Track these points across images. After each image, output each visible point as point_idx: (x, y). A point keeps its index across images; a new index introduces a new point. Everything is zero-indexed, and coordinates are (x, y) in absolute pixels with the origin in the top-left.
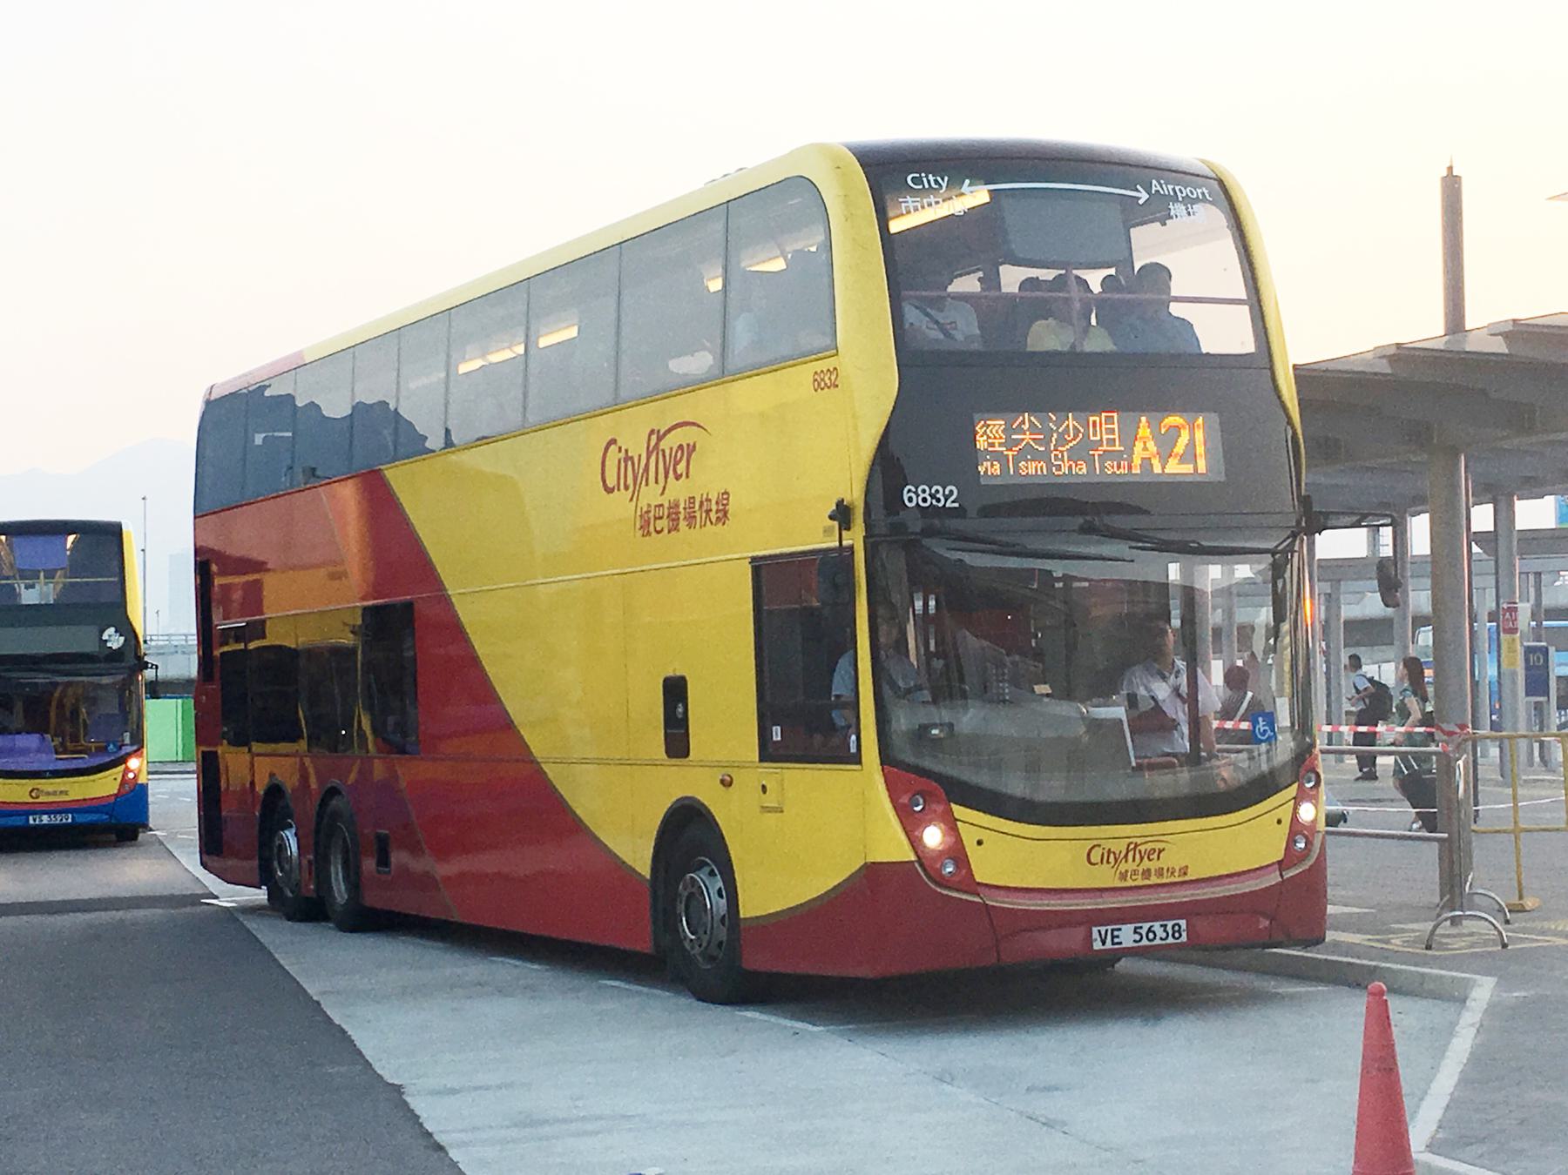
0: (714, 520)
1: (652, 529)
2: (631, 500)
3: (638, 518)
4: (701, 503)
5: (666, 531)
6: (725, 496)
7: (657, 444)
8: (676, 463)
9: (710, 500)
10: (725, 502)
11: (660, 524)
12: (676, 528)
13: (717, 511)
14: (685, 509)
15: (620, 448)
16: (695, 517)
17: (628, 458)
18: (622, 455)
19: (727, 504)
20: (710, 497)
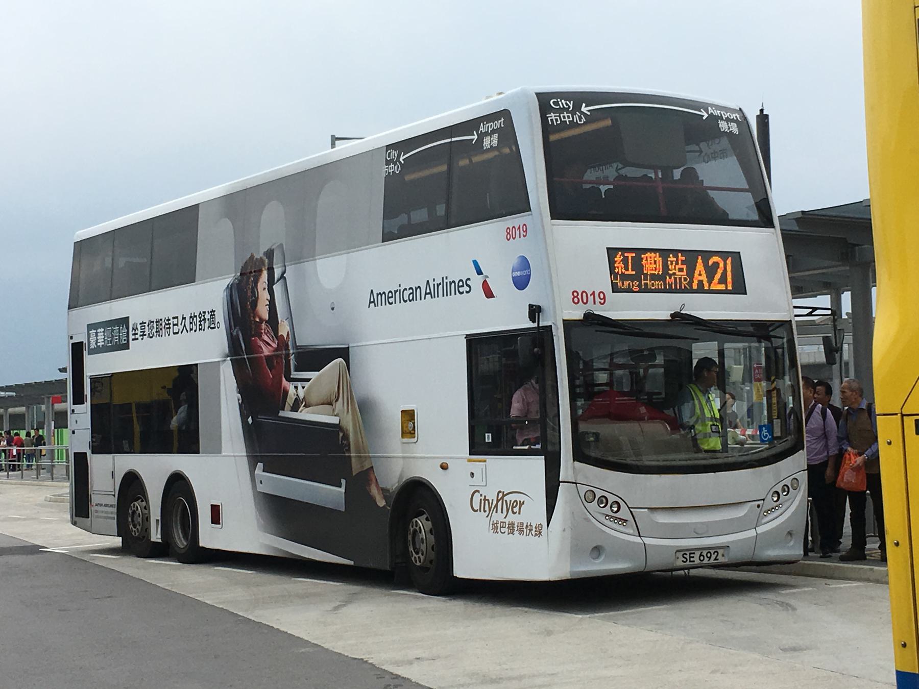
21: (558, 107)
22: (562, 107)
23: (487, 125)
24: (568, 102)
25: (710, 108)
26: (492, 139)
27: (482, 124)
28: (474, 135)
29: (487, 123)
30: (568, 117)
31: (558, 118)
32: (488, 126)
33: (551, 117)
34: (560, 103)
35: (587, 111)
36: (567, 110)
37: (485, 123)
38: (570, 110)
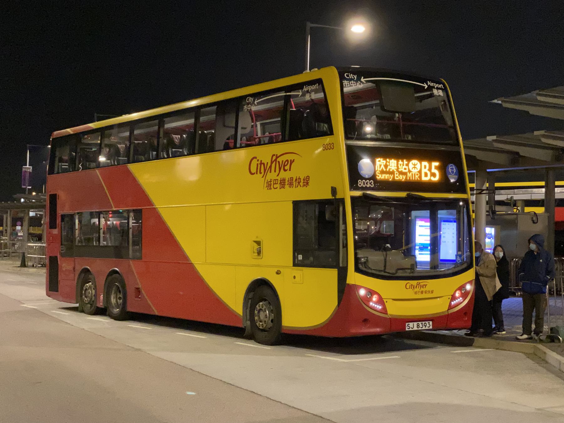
0: (302, 186)
1: (272, 187)
2: (263, 177)
3: (266, 184)
4: (296, 180)
5: (279, 188)
6: (307, 178)
7: (276, 160)
8: (285, 166)
9: (300, 179)
10: (307, 179)
11: (275, 186)
12: (284, 188)
13: (303, 183)
14: (288, 181)
15: (258, 160)
16: (293, 184)
17: (261, 163)
18: (259, 162)
19: (309, 180)
20: (300, 177)
21: (349, 78)
22: (351, 78)
23: (308, 87)
24: (354, 75)
25: (428, 82)
26: (311, 95)
27: (305, 86)
28: (299, 92)
29: (308, 86)
30: (354, 83)
31: (349, 83)
32: (309, 88)
33: (345, 82)
34: (350, 75)
35: (365, 81)
36: (353, 80)
37: (307, 86)
38: (355, 80)
